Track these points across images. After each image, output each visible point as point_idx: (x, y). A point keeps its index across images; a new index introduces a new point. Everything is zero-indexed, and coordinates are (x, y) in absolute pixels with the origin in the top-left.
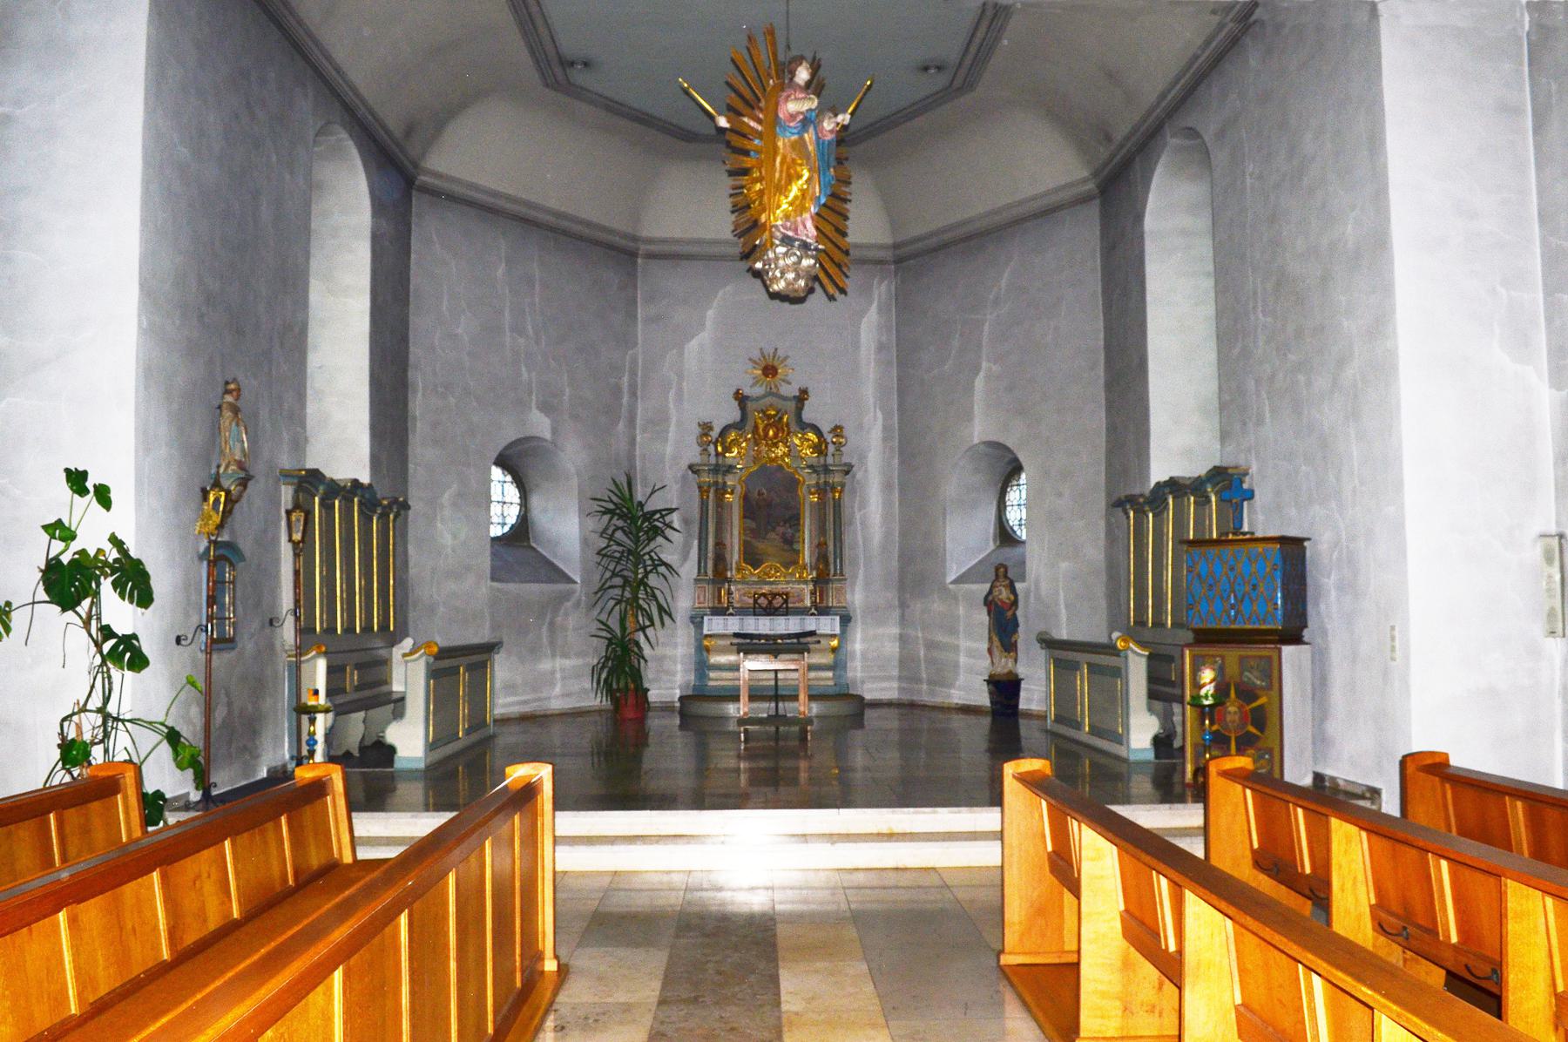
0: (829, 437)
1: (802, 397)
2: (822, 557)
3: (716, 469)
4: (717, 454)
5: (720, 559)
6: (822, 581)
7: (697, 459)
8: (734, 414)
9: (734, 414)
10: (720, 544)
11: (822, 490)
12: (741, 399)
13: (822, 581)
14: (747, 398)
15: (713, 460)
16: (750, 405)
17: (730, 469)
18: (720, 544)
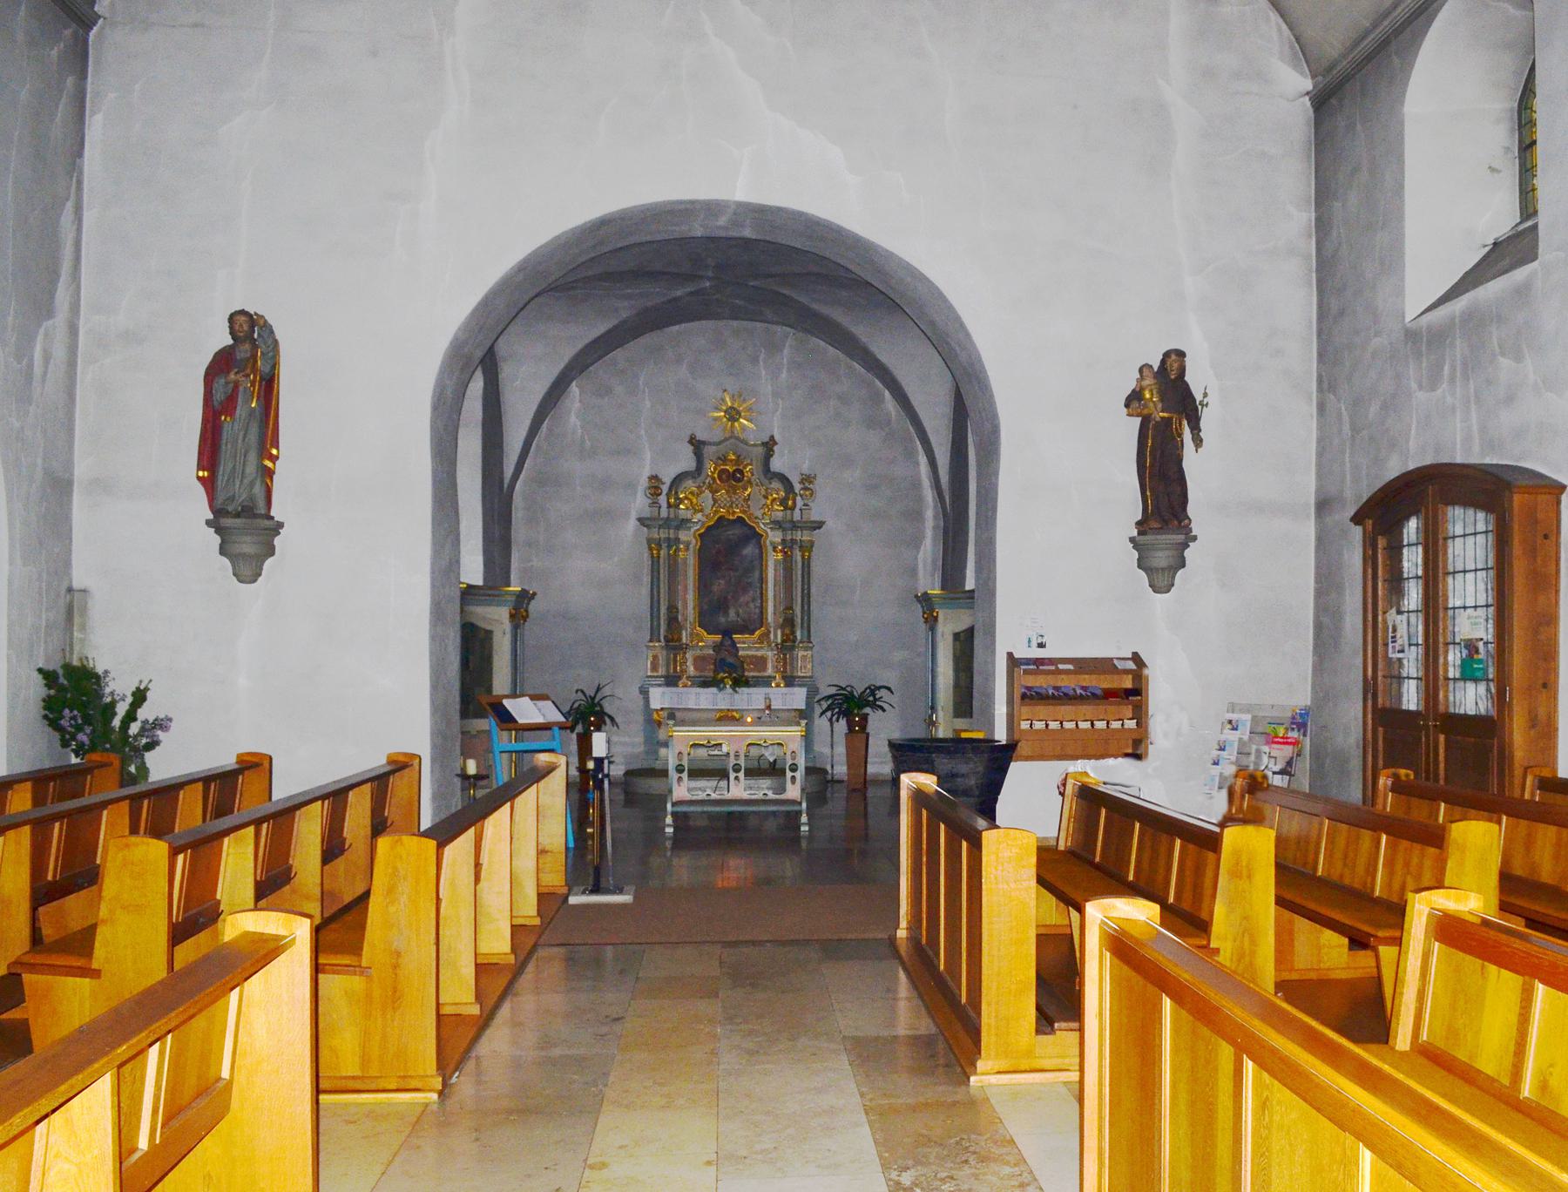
0: (797, 487)
1: (769, 446)
2: (789, 623)
3: (667, 523)
4: (669, 506)
5: (673, 621)
6: (787, 646)
7: (647, 513)
8: (686, 462)
9: (686, 462)
10: (672, 609)
11: (787, 546)
12: (697, 445)
13: (787, 646)
14: (704, 443)
15: (664, 513)
16: (709, 451)
17: (684, 523)
18: (672, 609)
